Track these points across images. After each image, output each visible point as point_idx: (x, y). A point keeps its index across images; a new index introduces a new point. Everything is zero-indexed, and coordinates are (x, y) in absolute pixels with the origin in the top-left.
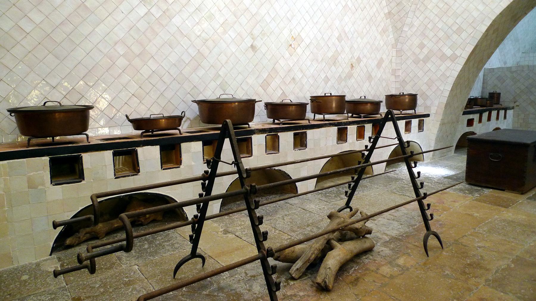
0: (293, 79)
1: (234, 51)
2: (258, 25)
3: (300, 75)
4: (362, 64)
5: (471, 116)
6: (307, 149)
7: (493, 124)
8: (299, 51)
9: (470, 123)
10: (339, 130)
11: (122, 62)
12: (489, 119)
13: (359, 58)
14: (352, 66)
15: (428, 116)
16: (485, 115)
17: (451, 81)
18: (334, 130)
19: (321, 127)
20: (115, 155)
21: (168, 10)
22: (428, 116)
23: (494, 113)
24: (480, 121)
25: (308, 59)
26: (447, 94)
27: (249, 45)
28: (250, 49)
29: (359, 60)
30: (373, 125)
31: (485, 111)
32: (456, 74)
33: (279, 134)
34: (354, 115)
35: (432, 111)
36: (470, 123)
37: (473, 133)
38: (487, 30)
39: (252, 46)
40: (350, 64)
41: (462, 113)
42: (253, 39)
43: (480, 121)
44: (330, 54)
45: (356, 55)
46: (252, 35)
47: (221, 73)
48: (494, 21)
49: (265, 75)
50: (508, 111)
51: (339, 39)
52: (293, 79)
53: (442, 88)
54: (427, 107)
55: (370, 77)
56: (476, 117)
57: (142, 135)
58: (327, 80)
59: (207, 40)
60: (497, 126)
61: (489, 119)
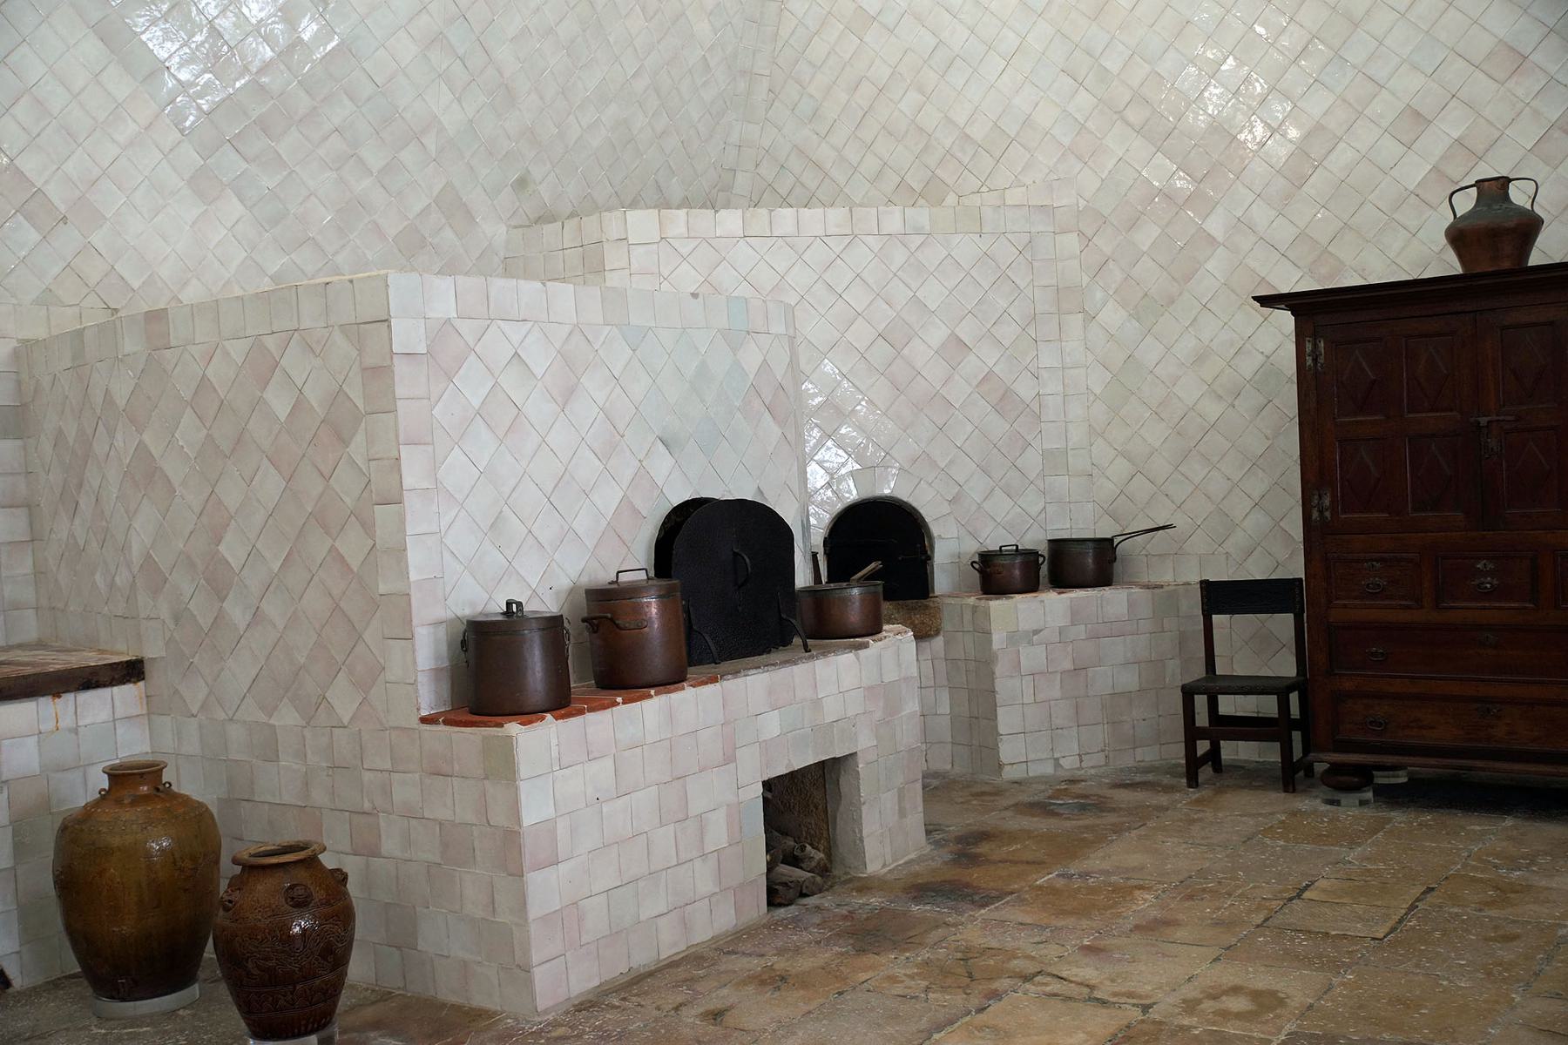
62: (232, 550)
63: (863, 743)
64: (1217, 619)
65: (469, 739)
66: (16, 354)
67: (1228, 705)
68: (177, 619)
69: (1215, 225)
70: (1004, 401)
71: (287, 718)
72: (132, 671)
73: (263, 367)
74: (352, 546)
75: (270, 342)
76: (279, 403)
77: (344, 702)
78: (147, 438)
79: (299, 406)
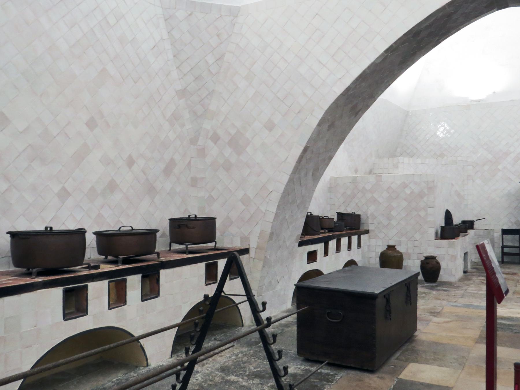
5: (312, 248)
7: (345, 256)
9: (312, 257)
10: (66, 293)
12: (338, 249)
13: (130, 157)
15: (246, 251)
16: (332, 244)
17: (276, 197)
18: (57, 293)
22: (246, 251)
23: (344, 241)
24: (326, 253)
26: (271, 217)
30: (143, 277)
31: (331, 238)
32: (282, 188)
34: (110, 258)
35: (253, 245)
36: (312, 257)
37: (317, 273)
38: (320, 124)
41: (297, 244)
43: (326, 253)
48: (327, 112)
50: (362, 237)
51: (91, 124)
53: (263, 209)
54: (244, 239)
55: (151, 190)
56: (319, 247)
60: (349, 259)
61: (338, 249)
62: (394, 213)
63: (468, 251)
64: (504, 236)
65: (445, 242)
66: (331, 179)
67: (506, 250)
68: (379, 223)
69: (500, 167)
70: (459, 195)
71: (404, 239)
72: (367, 232)
73: (405, 186)
74: (422, 214)
75: (407, 182)
76: (408, 191)
77: (417, 236)
78: (374, 195)
79: (412, 192)
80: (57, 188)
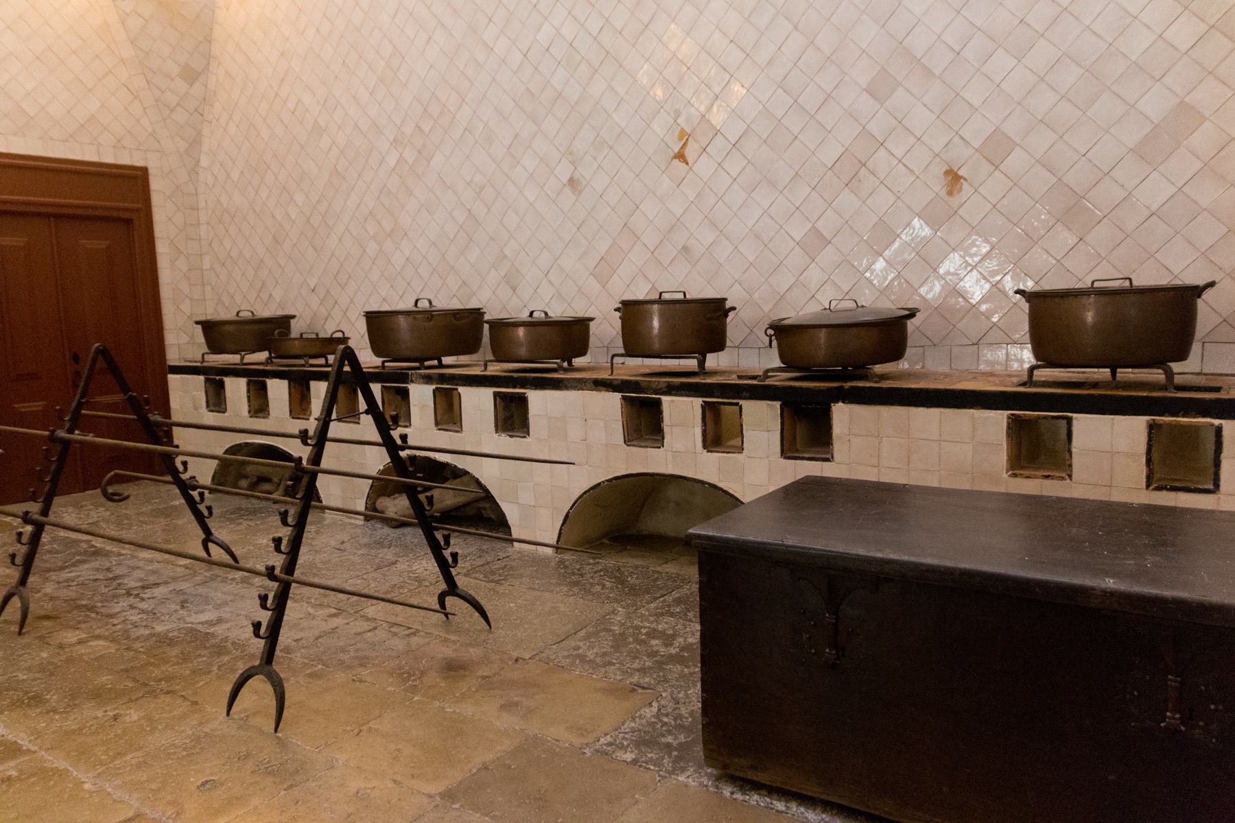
0: (685, 249)
1: (532, 199)
2: (586, 126)
3: (708, 236)
4: (1016, 161)
6: (529, 439)
8: (704, 166)
11: (372, 247)
14: (954, 179)
19: (567, 388)
20: (248, 384)
21: (424, 146)
25: (735, 187)
27: (565, 180)
28: (567, 190)
29: (996, 149)
33: (461, 389)
39: (572, 182)
40: (938, 170)
42: (573, 163)
44: (830, 154)
45: (977, 131)
46: (571, 153)
47: (507, 252)
49: (603, 247)
52: (685, 249)
57: (269, 361)
58: (816, 242)
59: (482, 188)
80: (798, 230)
